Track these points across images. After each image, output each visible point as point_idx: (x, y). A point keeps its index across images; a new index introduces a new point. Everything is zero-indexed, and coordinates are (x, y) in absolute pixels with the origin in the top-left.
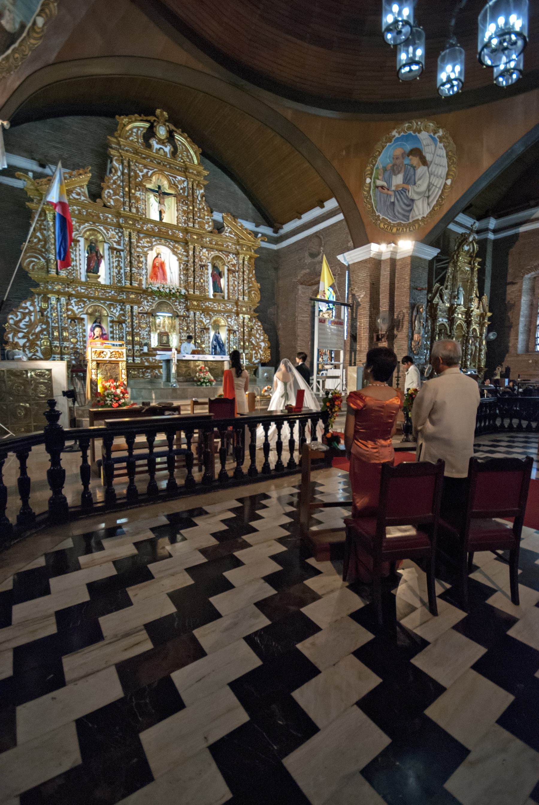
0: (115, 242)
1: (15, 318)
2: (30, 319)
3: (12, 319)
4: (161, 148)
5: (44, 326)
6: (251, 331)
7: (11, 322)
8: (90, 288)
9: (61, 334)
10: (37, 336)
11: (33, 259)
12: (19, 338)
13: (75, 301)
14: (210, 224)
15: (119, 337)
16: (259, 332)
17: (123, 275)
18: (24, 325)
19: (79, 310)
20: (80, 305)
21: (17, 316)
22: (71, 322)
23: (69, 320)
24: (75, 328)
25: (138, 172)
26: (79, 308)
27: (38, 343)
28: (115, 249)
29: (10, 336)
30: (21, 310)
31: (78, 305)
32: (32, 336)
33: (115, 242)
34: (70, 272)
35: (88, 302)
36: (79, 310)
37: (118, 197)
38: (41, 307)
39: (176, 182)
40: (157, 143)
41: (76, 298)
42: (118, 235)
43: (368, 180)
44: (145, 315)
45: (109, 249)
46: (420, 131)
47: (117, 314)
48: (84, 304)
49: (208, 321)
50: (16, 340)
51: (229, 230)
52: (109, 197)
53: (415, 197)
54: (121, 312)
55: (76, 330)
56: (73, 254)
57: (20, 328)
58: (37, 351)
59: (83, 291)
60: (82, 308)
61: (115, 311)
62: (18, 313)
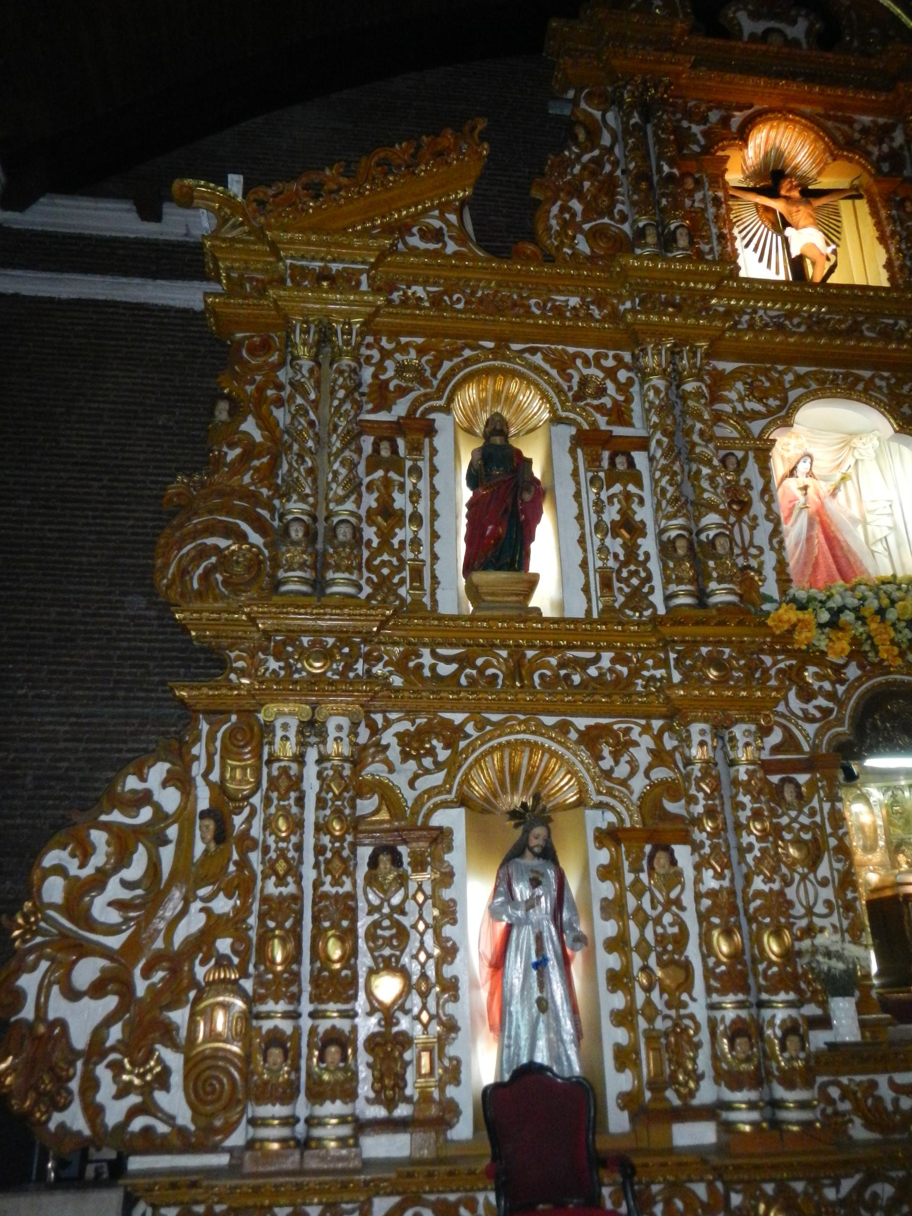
0: (600, 409)
2: (154, 866)
5: (223, 905)
10: (174, 972)
11: (211, 541)
12: (72, 995)
13: (397, 735)
15: (661, 939)
17: (654, 566)
19: (424, 783)
20: (432, 752)
21: (85, 852)
22: (373, 862)
24: (396, 900)
25: (685, 124)
27: (180, 1016)
28: (607, 440)
29: (29, 982)
30: (116, 816)
31: (418, 758)
32: (147, 973)
33: (600, 409)
34: (385, 580)
35: (470, 728)
36: (424, 783)
37: (606, 220)
39: (857, 136)
40: (755, 16)
41: (410, 714)
42: (615, 380)
44: (802, 778)
45: (572, 452)
47: (639, 784)
50: (58, 1006)
54: (660, 773)
56: (402, 487)
57: (91, 924)
58: (163, 1080)
59: (445, 669)
60: (438, 766)
61: (622, 770)
62: (98, 837)
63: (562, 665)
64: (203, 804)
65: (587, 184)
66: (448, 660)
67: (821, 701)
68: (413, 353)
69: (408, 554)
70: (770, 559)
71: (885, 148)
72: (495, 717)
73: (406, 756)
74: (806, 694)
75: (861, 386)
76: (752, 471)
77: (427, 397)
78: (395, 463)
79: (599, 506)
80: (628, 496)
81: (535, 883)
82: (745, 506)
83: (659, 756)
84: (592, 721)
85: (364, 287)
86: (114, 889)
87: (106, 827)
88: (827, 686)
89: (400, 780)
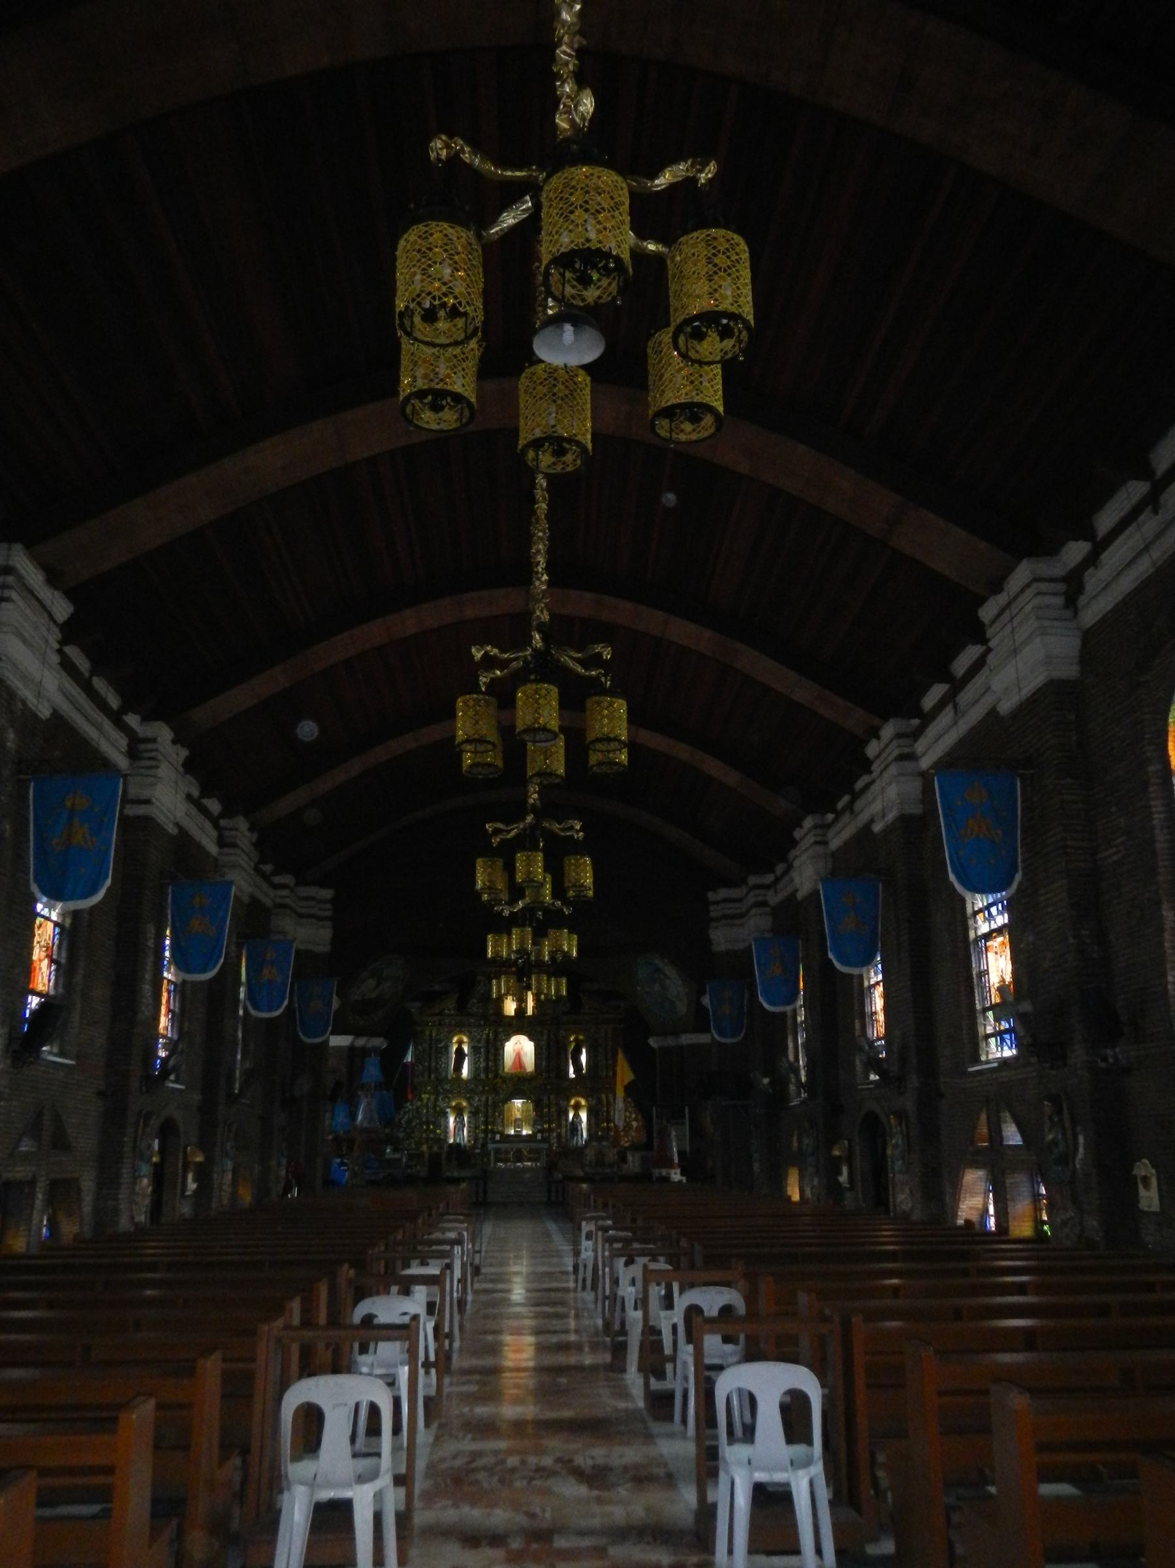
5: (418, 1121)
16: (630, 1109)
43: (639, 988)
74: (503, 1090)
76: (501, 1052)
83: (479, 1100)
86: (404, 1120)
89: (441, 1104)
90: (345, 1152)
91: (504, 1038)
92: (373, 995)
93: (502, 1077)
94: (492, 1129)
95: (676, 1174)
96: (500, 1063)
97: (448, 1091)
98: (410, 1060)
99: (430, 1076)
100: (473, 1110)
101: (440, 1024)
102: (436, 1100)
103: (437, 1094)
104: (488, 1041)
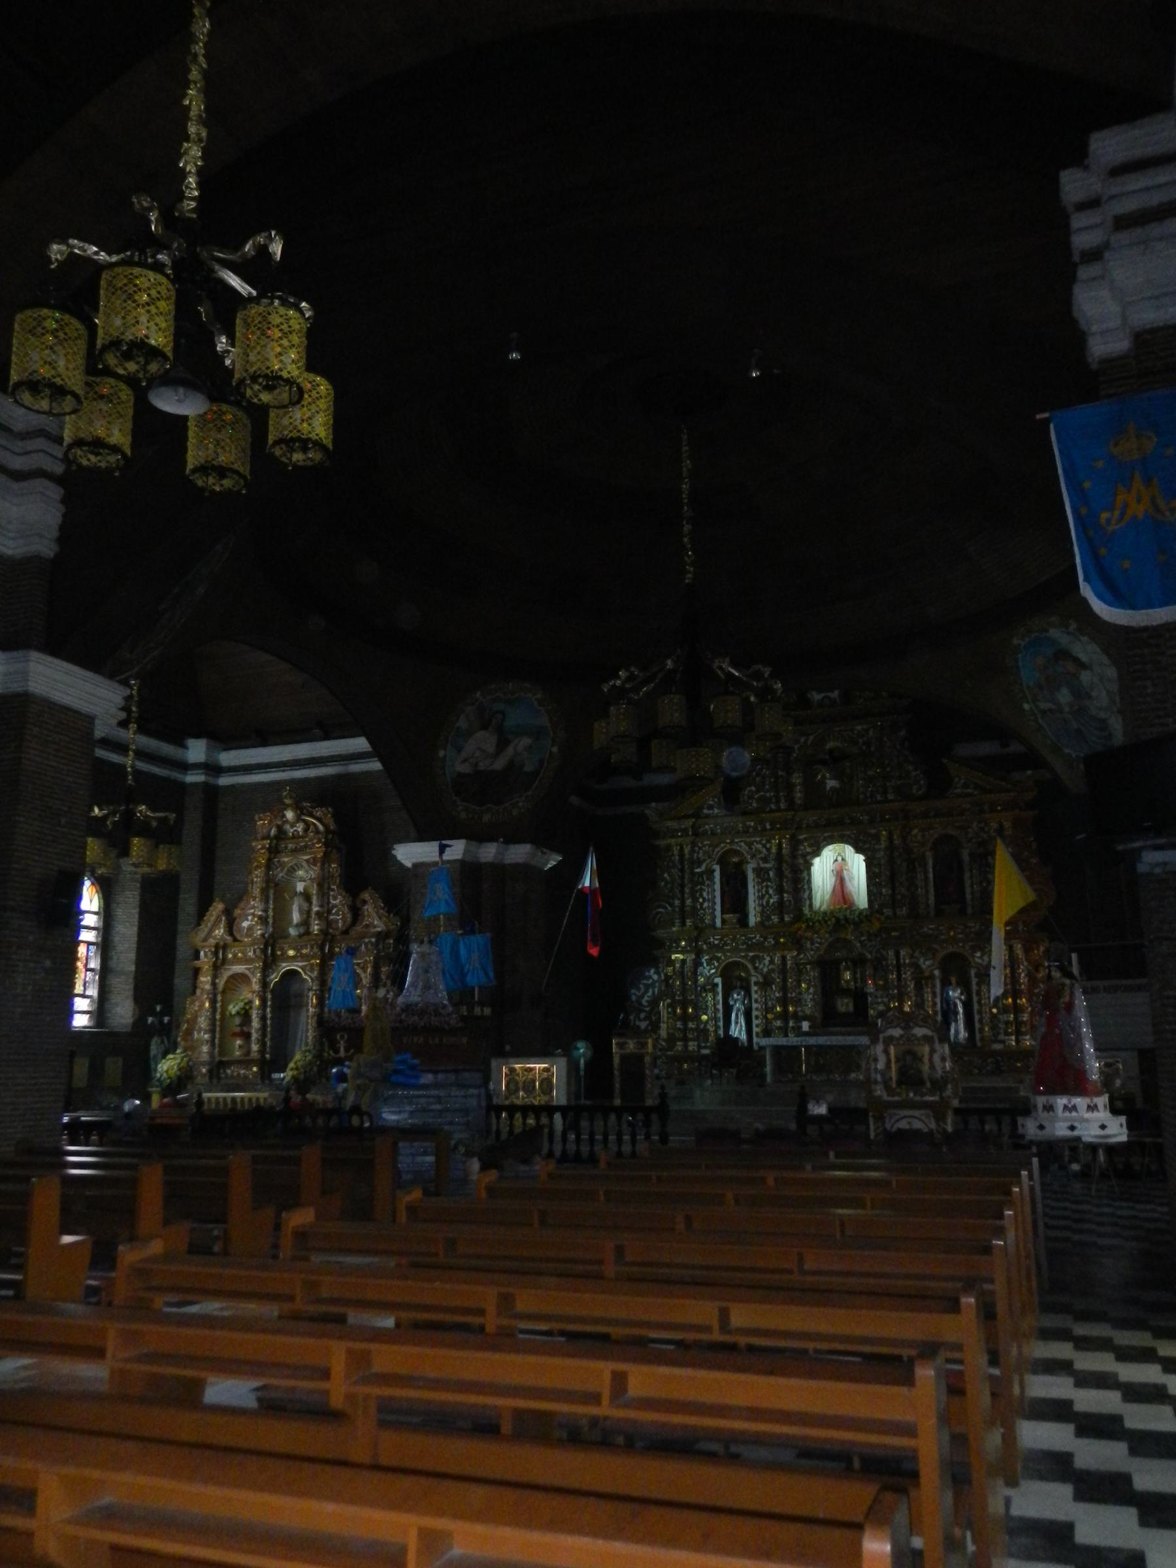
0: (762, 859)
1: (637, 993)
3: (634, 993)
4: (823, 698)
6: (1037, 970)
7: (634, 998)
8: (727, 936)
9: (685, 1010)
11: (659, 910)
12: (640, 1020)
14: (922, 782)
18: (647, 1001)
20: (714, 964)
21: (639, 989)
23: (699, 988)
26: (712, 969)
28: (762, 869)
30: (645, 982)
33: (762, 859)
35: (723, 958)
37: (762, 793)
38: (666, 975)
41: (708, 954)
43: (1026, 706)
44: (808, 967)
46: (1047, 631)
47: (765, 970)
48: (718, 962)
49: (928, 963)
50: (638, 1023)
51: (962, 781)
52: (751, 797)
53: (1102, 715)
54: (771, 967)
55: (707, 1002)
57: (641, 1004)
59: (716, 942)
61: (761, 966)
62: (641, 986)
63: (746, 939)
64: (663, 978)
65: (757, 779)
66: (716, 939)
67: (817, 945)
68: (707, 847)
69: (707, 911)
70: (808, 902)
71: (865, 739)
72: (729, 954)
73: (707, 965)
74: (812, 944)
75: (845, 839)
76: (805, 874)
77: (711, 862)
78: (703, 884)
79: (759, 891)
80: (767, 887)
81: (738, 995)
82: (803, 886)
83: (772, 962)
84: (753, 954)
85: (690, 833)
86: (646, 998)
87: (643, 984)
88: (819, 940)
89: (706, 971)
90: (342, 1053)
91: (809, 850)
92: (499, 764)
93: (807, 920)
94: (795, 1013)
95: (1092, 1108)
96: (806, 895)
97: (712, 947)
98: (587, 884)
99: (683, 924)
100: (761, 980)
101: (696, 834)
102: (697, 964)
103: (699, 953)
104: (779, 857)
